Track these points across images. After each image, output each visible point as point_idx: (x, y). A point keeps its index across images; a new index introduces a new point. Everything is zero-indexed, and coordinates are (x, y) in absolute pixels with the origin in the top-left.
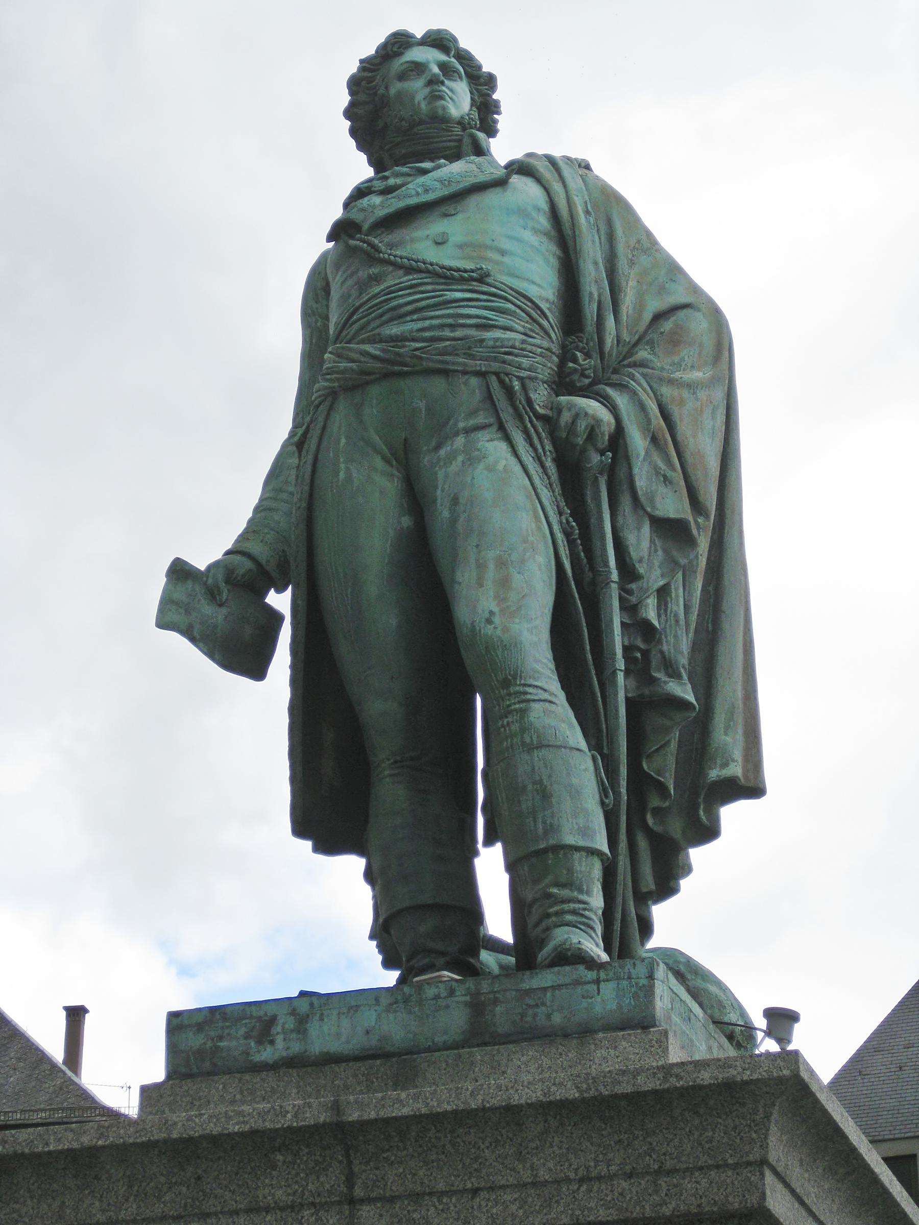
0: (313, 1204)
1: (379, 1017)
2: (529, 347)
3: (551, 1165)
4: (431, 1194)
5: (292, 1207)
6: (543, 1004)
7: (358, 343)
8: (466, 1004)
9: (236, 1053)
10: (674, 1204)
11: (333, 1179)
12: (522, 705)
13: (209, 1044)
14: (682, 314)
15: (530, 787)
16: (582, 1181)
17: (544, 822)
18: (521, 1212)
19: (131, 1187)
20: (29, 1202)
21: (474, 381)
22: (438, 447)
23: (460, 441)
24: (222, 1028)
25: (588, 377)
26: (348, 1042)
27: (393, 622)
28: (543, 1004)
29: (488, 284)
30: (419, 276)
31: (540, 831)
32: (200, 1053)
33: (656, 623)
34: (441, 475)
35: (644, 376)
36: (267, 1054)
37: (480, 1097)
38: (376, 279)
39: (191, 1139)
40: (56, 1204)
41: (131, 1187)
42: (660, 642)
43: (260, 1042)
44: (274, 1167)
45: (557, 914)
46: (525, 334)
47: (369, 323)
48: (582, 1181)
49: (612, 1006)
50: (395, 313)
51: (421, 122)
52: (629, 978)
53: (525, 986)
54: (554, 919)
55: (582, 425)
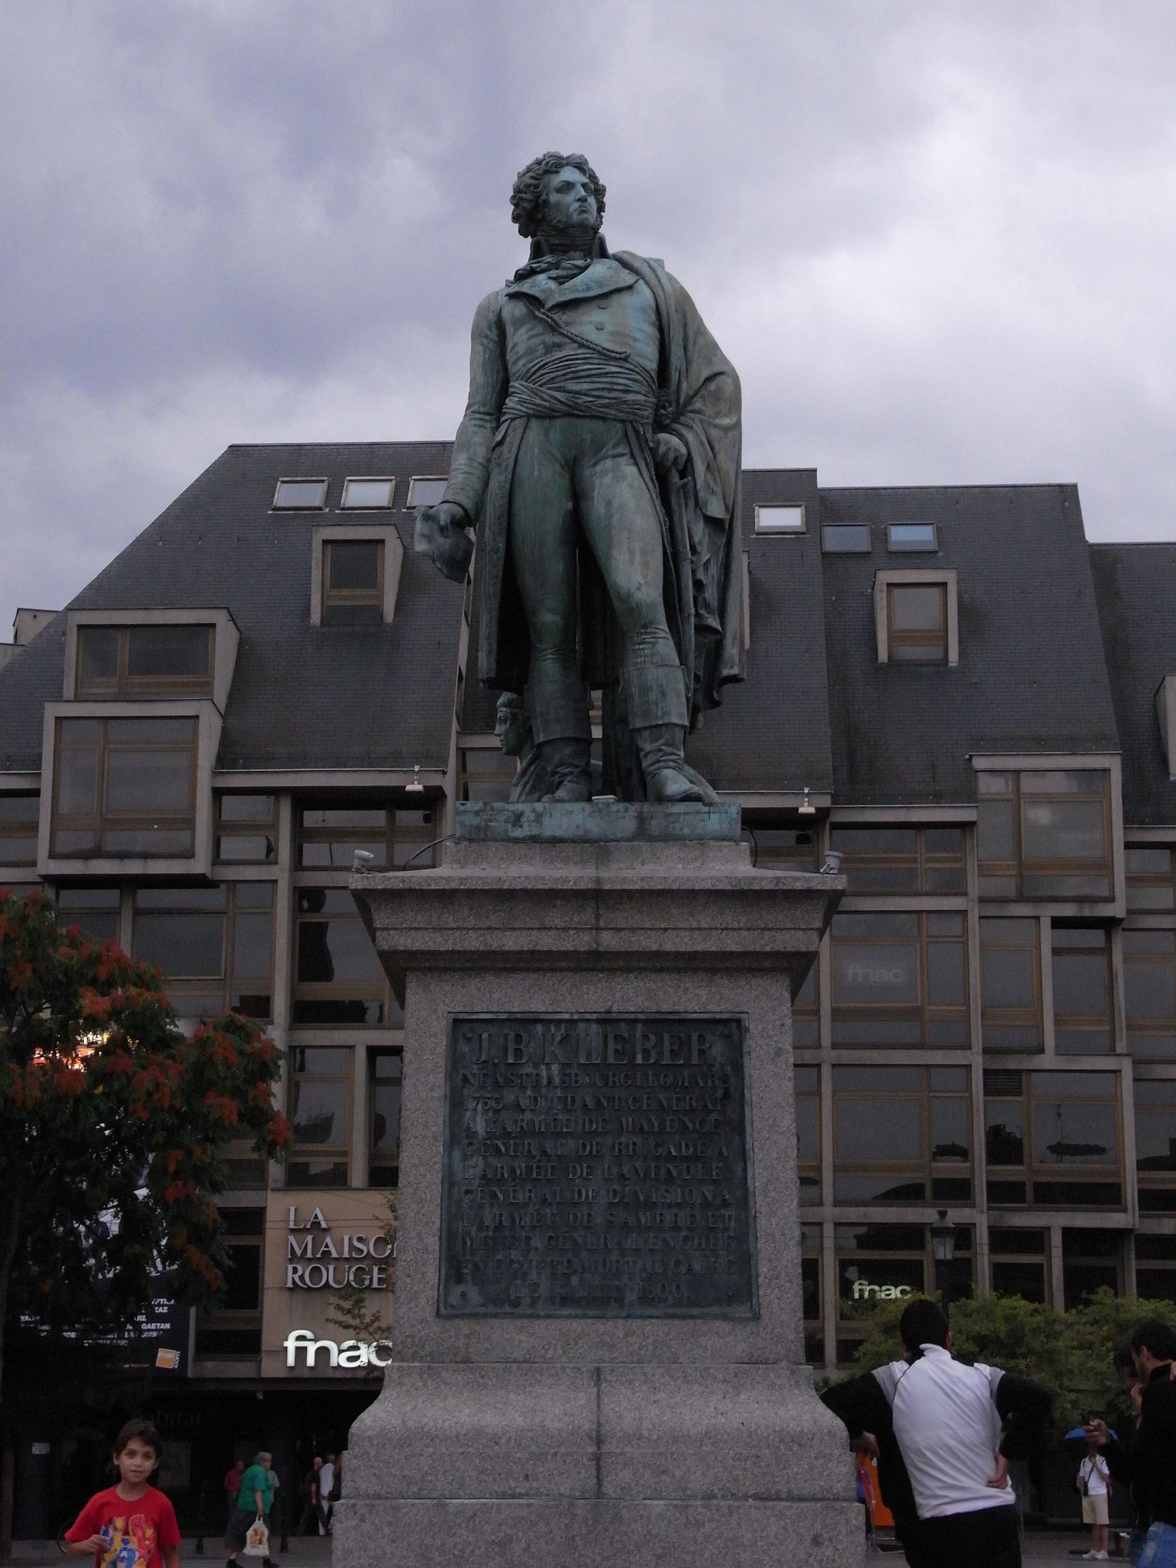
0: (575, 929)
5: (564, 929)
8: (635, 817)
13: (483, 824)
14: (720, 378)
15: (655, 688)
16: (723, 930)
18: (690, 942)
19: (471, 910)
20: (410, 913)
21: (619, 426)
22: (595, 464)
23: (609, 463)
27: (561, 567)
30: (587, 351)
31: (660, 714)
32: (478, 828)
34: (597, 483)
35: (701, 420)
36: (517, 833)
37: (678, 884)
38: (559, 346)
39: (515, 890)
41: (471, 910)
43: (514, 825)
44: (555, 907)
45: (664, 761)
47: (557, 376)
48: (723, 930)
49: (716, 827)
50: (575, 375)
51: (573, 226)
52: (727, 813)
53: (669, 811)
54: (661, 764)
55: (671, 456)
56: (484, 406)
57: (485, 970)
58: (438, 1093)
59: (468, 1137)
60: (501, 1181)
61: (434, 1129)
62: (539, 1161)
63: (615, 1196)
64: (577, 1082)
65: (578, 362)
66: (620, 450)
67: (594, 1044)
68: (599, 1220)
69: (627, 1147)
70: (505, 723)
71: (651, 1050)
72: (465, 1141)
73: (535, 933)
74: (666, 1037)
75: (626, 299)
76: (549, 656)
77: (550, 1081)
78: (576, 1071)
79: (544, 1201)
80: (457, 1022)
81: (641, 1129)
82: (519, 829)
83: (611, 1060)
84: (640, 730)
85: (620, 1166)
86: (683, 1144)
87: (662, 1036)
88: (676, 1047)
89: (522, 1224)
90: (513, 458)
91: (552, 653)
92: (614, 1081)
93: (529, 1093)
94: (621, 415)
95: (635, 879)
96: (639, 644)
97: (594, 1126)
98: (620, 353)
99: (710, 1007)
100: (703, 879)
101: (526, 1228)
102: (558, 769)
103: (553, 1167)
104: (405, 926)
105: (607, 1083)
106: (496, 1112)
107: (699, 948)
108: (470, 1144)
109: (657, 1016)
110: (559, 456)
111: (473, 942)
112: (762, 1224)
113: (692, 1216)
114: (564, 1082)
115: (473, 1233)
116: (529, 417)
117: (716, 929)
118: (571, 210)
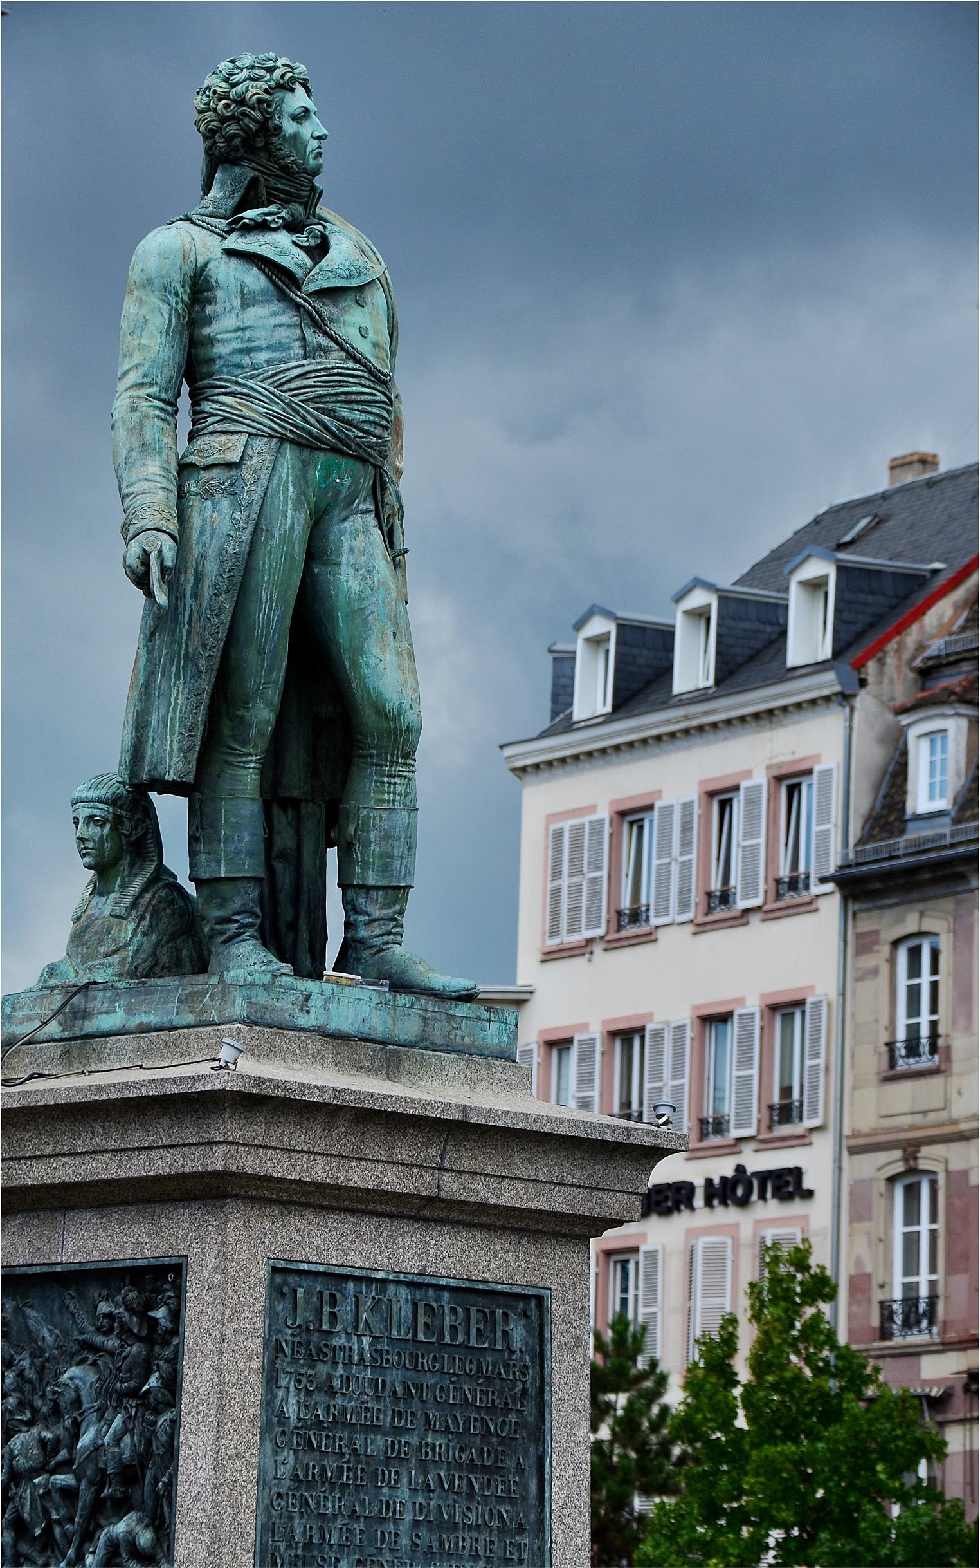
3: (545, 1170)
4: (481, 1174)
10: (598, 1211)
11: (435, 1151)
17: (406, 866)
19: (324, 1130)
22: (345, 520)
28: (461, 1029)
30: (357, 366)
36: (303, 1021)
40: (280, 1131)
45: (395, 934)
50: (348, 397)
53: (452, 1012)
54: (391, 937)
56: (166, 392)
57: (307, 1205)
58: (256, 1364)
59: (280, 1423)
60: (310, 1485)
61: (251, 1410)
62: (348, 1462)
63: (421, 1512)
64: (387, 1360)
65: (351, 380)
67: (403, 1314)
68: (405, 1541)
69: (433, 1449)
70: (102, 826)
71: (459, 1327)
72: (278, 1430)
73: (379, 1166)
74: (473, 1310)
76: (252, 765)
77: (362, 1359)
78: (386, 1347)
79: (353, 1515)
80: (275, 1270)
81: (448, 1427)
83: (421, 1336)
84: (368, 888)
85: (426, 1476)
86: (486, 1449)
87: (468, 1310)
88: (481, 1326)
89: (332, 1542)
90: (260, 491)
92: (423, 1363)
93: (340, 1370)
95: (500, 1113)
96: (390, 776)
97: (403, 1421)
99: (518, 1279)
100: (562, 1121)
101: (335, 1547)
102: (237, 917)
103: (362, 1469)
104: (256, 1142)
105: (416, 1366)
106: (309, 1393)
107: (533, 1205)
108: (283, 1432)
109: (468, 1284)
111: (319, 1172)
112: (557, 1555)
113: (492, 1542)
114: (374, 1360)
115: (282, 1549)
116: (283, 439)
117: (551, 1183)
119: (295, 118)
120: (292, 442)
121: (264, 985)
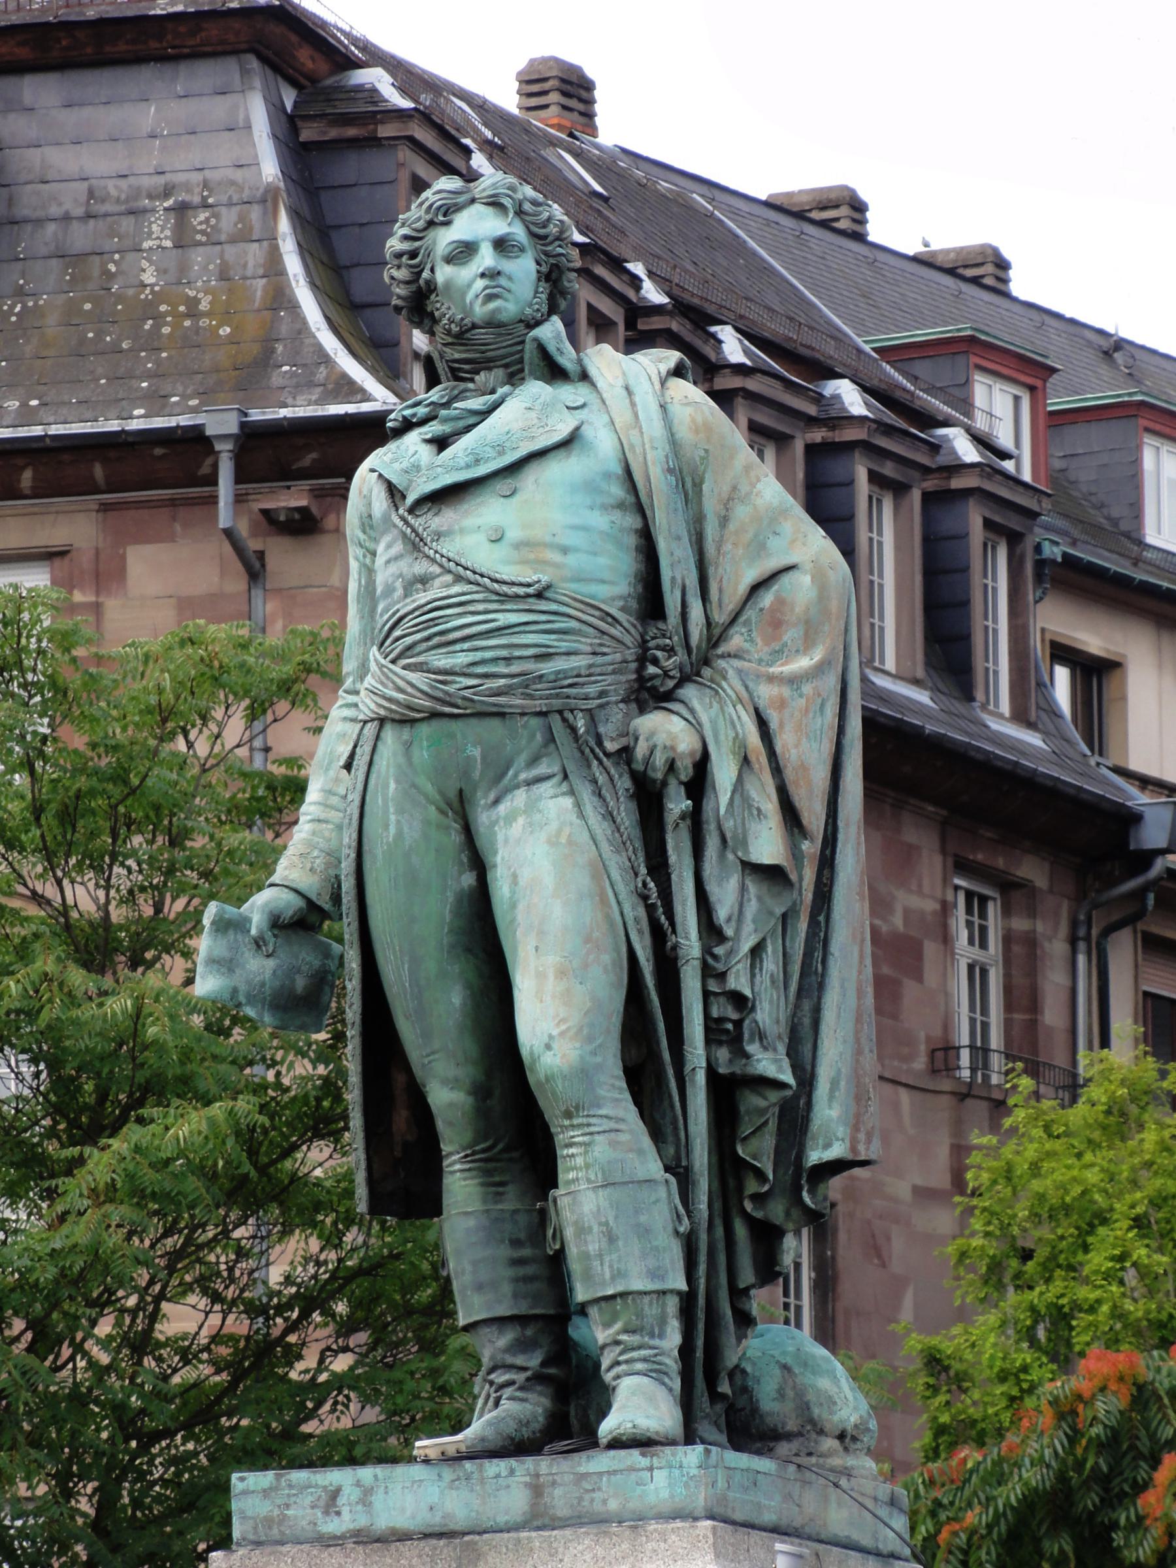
1: (442, 1493)
2: (598, 670)
6: (599, 1489)
7: (404, 668)
8: (526, 1485)
9: (304, 1523)
12: (586, 1139)
13: (276, 1512)
14: (786, 580)
15: (596, 1229)
17: (611, 1266)
21: (534, 722)
22: (497, 802)
23: (520, 797)
24: (289, 1496)
25: (672, 678)
26: (413, 1518)
29: (547, 599)
31: (608, 1276)
32: (268, 1521)
33: (747, 992)
34: (500, 837)
35: (739, 672)
36: (332, 1526)
38: (424, 581)
42: (753, 1009)
43: (326, 1513)
45: (627, 1362)
46: (594, 653)
49: (665, 1494)
50: (443, 639)
51: (474, 326)
53: (582, 1469)
54: (623, 1367)
55: (659, 760)
66: (542, 769)
75: (555, 470)
82: (336, 1520)
91: (460, 1161)
94: (540, 705)
98: (529, 585)
110: (429, 788)
116: (382, 721)
118: (470, 296)
119: (449, 260)
120: (393, 720)
121: (264, 1491)
